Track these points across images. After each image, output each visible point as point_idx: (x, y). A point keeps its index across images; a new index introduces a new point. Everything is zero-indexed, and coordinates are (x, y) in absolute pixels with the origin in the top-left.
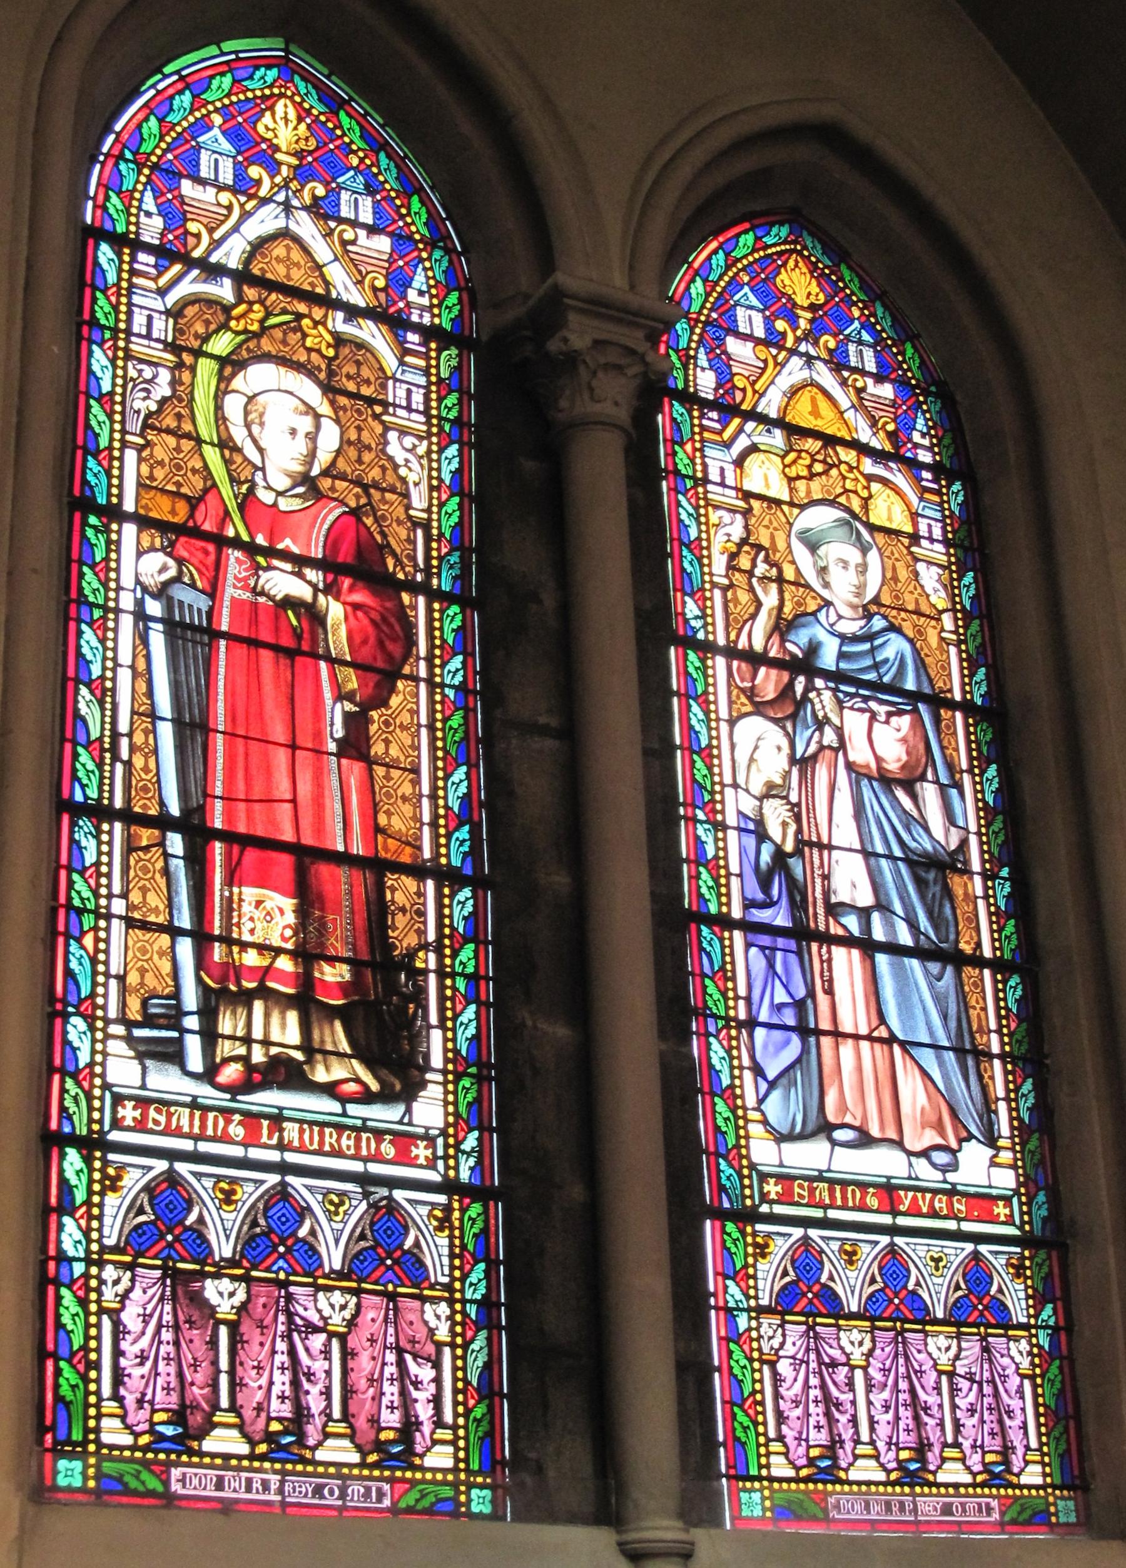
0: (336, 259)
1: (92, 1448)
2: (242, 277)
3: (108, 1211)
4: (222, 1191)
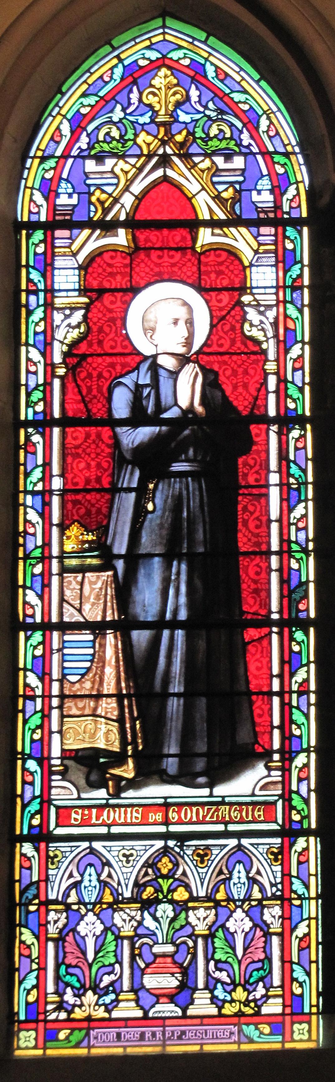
0: (203, 189)
2: (131, 224)
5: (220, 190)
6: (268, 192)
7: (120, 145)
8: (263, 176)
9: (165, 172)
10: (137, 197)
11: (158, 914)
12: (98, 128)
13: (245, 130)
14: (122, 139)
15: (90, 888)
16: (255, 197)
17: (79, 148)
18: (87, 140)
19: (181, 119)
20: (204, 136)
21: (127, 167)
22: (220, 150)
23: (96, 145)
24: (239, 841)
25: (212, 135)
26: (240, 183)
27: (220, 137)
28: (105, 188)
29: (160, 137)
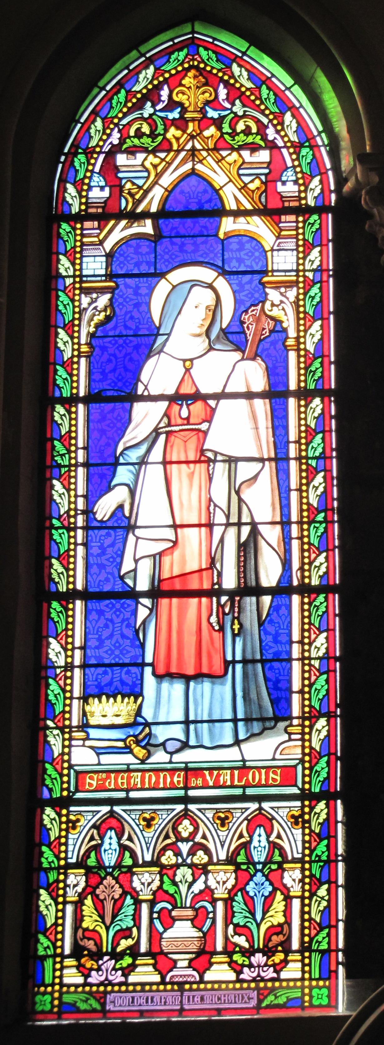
0: (231, 181)
1: (57, 987)
3: (71, 842)
4: (145, 819)
5: (247, 182)
6: (292, 183)
7: (150, 140)
8: (287, 168)
9: (194, 165)
10: (166, 190)
11: (177, 879)
12: (130, 124)
13: (270, 125)
14: (153, 135)
15: (110, 851)
16: (280, 187)
17: (111, 143)
18: (119, 135)
19: (209, 115)
20: (230, 131)
21: (157, 161)
22: (246, 144)
23: (128, 140)
24: (260, 805)
25: (239, 130)
26: (266, 175)
27: (247, 132)
28: (136, 181)
29: (189, 131)
